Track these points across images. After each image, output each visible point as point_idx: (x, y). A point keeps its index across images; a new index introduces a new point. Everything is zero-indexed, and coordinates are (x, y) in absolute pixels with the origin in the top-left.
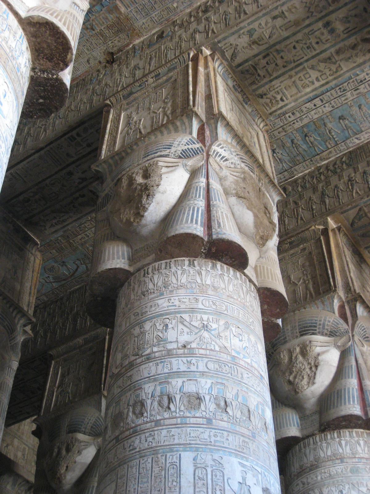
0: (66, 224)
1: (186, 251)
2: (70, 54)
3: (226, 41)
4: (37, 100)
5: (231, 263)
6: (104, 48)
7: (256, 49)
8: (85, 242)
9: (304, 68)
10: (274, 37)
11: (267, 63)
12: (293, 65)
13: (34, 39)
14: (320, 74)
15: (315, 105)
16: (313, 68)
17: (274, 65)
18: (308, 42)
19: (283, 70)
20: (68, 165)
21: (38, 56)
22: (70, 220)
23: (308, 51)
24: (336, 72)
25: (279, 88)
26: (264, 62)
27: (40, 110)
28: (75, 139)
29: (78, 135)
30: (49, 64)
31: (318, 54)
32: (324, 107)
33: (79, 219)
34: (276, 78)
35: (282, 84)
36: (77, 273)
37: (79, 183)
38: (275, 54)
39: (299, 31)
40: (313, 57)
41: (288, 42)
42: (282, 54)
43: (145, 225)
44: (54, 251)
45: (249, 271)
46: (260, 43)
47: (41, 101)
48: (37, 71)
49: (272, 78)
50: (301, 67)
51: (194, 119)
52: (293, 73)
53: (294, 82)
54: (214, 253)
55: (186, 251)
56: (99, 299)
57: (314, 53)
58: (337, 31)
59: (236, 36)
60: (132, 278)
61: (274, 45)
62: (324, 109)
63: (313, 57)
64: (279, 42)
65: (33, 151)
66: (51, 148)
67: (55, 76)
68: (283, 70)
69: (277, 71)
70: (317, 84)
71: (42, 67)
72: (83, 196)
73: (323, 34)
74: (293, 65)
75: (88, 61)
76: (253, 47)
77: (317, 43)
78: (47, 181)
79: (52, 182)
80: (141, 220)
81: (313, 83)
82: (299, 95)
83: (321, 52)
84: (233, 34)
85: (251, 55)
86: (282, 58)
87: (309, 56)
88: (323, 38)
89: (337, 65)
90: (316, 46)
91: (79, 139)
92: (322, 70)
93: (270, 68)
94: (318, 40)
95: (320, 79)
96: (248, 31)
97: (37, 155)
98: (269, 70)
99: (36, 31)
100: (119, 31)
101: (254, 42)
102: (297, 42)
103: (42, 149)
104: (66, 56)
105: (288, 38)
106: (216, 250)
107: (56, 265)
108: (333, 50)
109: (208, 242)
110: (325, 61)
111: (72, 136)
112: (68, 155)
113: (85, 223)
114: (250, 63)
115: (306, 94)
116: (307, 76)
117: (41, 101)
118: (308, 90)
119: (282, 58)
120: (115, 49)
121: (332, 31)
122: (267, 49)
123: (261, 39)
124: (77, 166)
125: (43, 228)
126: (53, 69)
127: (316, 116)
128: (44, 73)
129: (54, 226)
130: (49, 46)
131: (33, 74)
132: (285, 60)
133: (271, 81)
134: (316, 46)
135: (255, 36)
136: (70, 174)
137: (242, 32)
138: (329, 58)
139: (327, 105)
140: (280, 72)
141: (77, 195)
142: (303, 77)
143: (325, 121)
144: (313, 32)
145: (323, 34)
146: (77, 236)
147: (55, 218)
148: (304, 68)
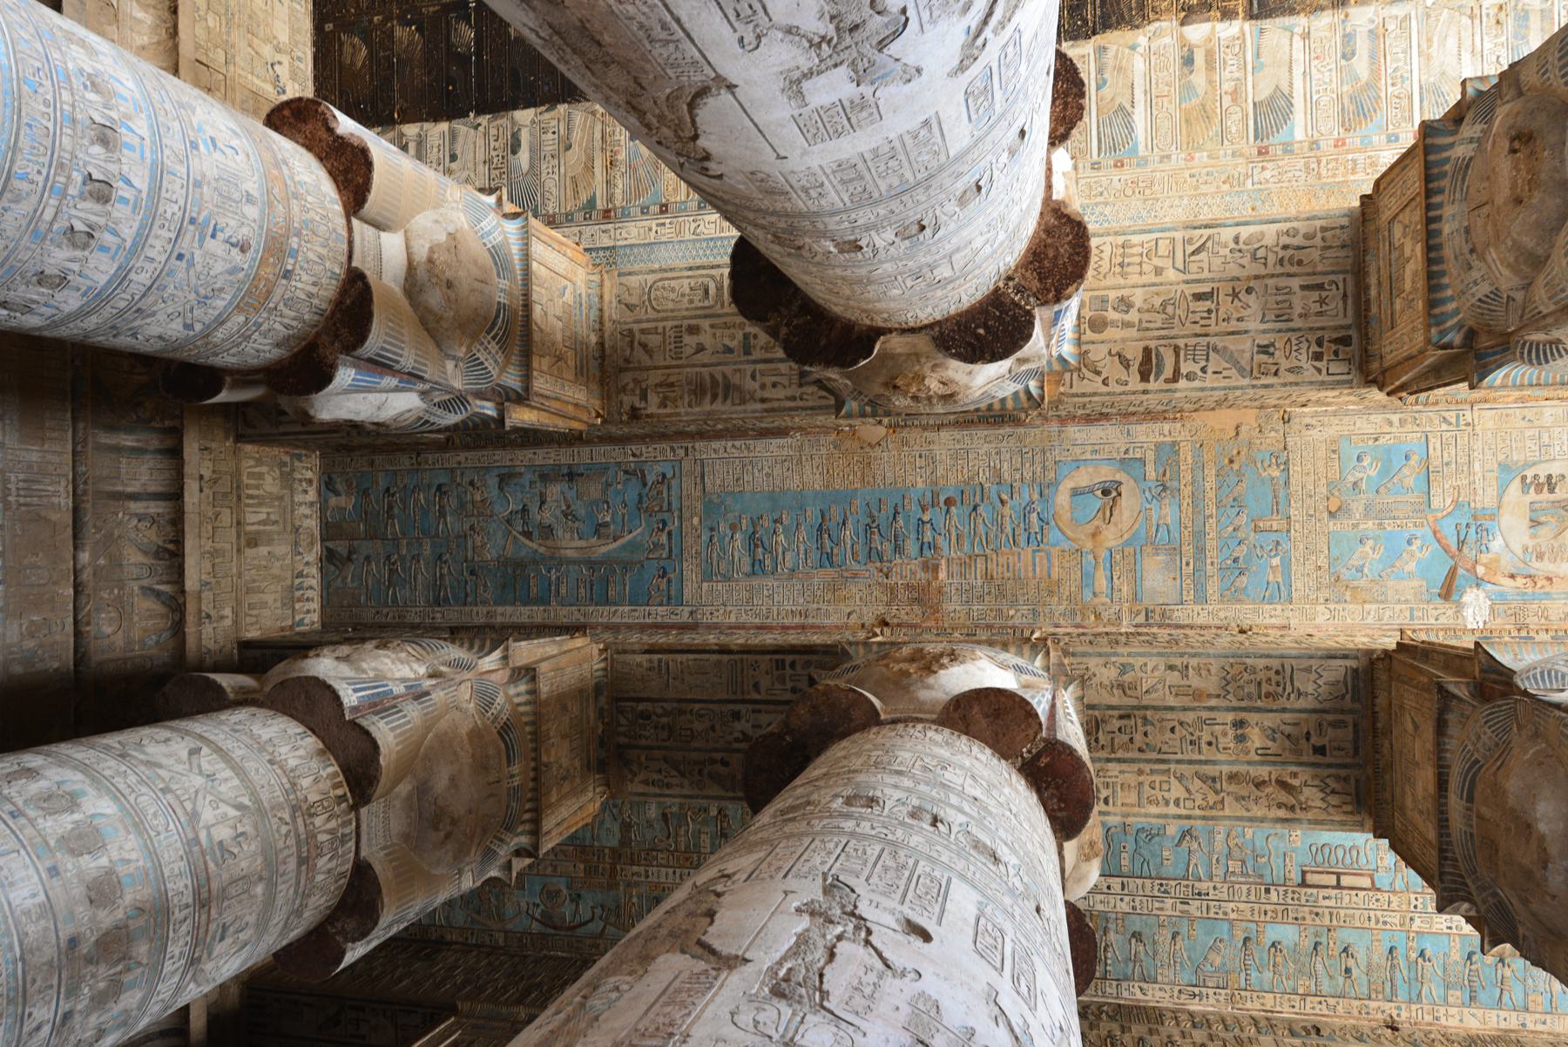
0: (667, 792)
1: (997, 735)
2: (1075, 285)
3: (1084, 660)
4: (978, 327)
5: (1053, 810)
6: (881, 609)
7: (1116, 699)
8: (637, 884)
9: (1169, 770)
10: (1154, 695)
11: (1120, 729)
12: (1154, 755)
13: (1044, 236)
14: (1187, 796)
15: (1109, 888)
16: (1180, 779)
17: (1126, 738)
18: (1198, 733)
19: (1137, 755)
20: (744, 701)
21: (1031, 262)
22: (677, 791)
23: (1190, 748)
24: (1211, 808)
25: (1114, 780)
26: (1116, 724)
27: (970, 344)
28: (784, 669)
29: (793, 665)
30: (1035, 285)
31: (1200, 762)
32: (1122, 900)
33: (690, 797)
34: (1119, 760)
35: (1121, 776)
36: (581, 931)
37: (737, 740)
38: (1139, 722)
39: (1194, 709)
40: (1191, 762)
41: (1169, 715)
42: (1149, 728)
43: (929, 687)
44: (582, 866)
45: (1070, 847)
46: (1128, 692)
47: (981, 331)
48: (1011, 284)
49: (1113, 756)
50: (1164, 767)
51: (1040, 657)
52: (1147, 768)
53: (1140, 784)
54: (1039, 768)
55: (997, 735)
56: (788, 738)
57: (1196, 757)
58: (1249, 744)
59: (1101, 660)
60: (875, 729)
61: (1146, 708)
62: (1118, 902)
63: (1191, 762)
64: (1155, 708)
65: (716, 648)
66: (742, 660)
67: (1028, 307)
68: (1137, 755)
69: (1128, 750)
70: (1172, 810)
71: (1023, 283)
72: (725, 763)
73: (1225, 734)
74: (1154, 755)
75: (849, 614)
76: (1115, 690)
77: (1210, 744)
78: (697, 706)
79: (702, 712)
80: (928, 676)
81: (1167, 803)
82: (1136, 809)
83: (1206, 762)
84: (1100, 655)
85: (1104, 702)
86: (1146, 734)
87: (1185, 757)
88: (1223, 742)
89: (1220, 798)
90: (1204, 746)
91: (788, 671)
92: (1193, 791)
93: (1123, 738)
94: (1214, 741)
95: (1182, 804)
96: (1122, 665)
97: (715, 657)
98: (1116, 741)
99: (1054, 226)
100: (918, 601)
101: (1121, 686)
102: (1181, 724)
103: (730, 652)
104: (1068, 285)
105: (1172, 709)
106: (1047, 765)
107: (565, 891)
108: (1226, 769)
109: (1044, 740)
110: (1204, 778)
111: (783, 661)
112: (756, 686)
113: (661, 851)
114: (1096, 713)
115: (1146, 815)
116: (1165, 787)
117: (981, 331)
118: (1153, 810)
119: (1146, 734)
120: (895, 621)
121: (1241, 739)
122: (1133, 707)
123: (1132, 686)
124: (754, 711)
125: (630, 777)
126: (1035, 295)
127: (1100, 907)
129: (648, 784)
130: (1056, 257)
131: (1001, 284)
132: (1147, 740)
133: (1108, 760)
134: (1204, 746)
135: (1127, 678)
136: (736, 716)
137: (1113, 659)
138: (1214, 779)
139: (1126, 899)
140: (1129, 755)
141: (718, 756)
142: (1157, 784)
143: (1110, 925)
144: (1211, 722)
145: (1225, 734)
146: (633, 864)
147: (660, 771)
148: (1169, 770)
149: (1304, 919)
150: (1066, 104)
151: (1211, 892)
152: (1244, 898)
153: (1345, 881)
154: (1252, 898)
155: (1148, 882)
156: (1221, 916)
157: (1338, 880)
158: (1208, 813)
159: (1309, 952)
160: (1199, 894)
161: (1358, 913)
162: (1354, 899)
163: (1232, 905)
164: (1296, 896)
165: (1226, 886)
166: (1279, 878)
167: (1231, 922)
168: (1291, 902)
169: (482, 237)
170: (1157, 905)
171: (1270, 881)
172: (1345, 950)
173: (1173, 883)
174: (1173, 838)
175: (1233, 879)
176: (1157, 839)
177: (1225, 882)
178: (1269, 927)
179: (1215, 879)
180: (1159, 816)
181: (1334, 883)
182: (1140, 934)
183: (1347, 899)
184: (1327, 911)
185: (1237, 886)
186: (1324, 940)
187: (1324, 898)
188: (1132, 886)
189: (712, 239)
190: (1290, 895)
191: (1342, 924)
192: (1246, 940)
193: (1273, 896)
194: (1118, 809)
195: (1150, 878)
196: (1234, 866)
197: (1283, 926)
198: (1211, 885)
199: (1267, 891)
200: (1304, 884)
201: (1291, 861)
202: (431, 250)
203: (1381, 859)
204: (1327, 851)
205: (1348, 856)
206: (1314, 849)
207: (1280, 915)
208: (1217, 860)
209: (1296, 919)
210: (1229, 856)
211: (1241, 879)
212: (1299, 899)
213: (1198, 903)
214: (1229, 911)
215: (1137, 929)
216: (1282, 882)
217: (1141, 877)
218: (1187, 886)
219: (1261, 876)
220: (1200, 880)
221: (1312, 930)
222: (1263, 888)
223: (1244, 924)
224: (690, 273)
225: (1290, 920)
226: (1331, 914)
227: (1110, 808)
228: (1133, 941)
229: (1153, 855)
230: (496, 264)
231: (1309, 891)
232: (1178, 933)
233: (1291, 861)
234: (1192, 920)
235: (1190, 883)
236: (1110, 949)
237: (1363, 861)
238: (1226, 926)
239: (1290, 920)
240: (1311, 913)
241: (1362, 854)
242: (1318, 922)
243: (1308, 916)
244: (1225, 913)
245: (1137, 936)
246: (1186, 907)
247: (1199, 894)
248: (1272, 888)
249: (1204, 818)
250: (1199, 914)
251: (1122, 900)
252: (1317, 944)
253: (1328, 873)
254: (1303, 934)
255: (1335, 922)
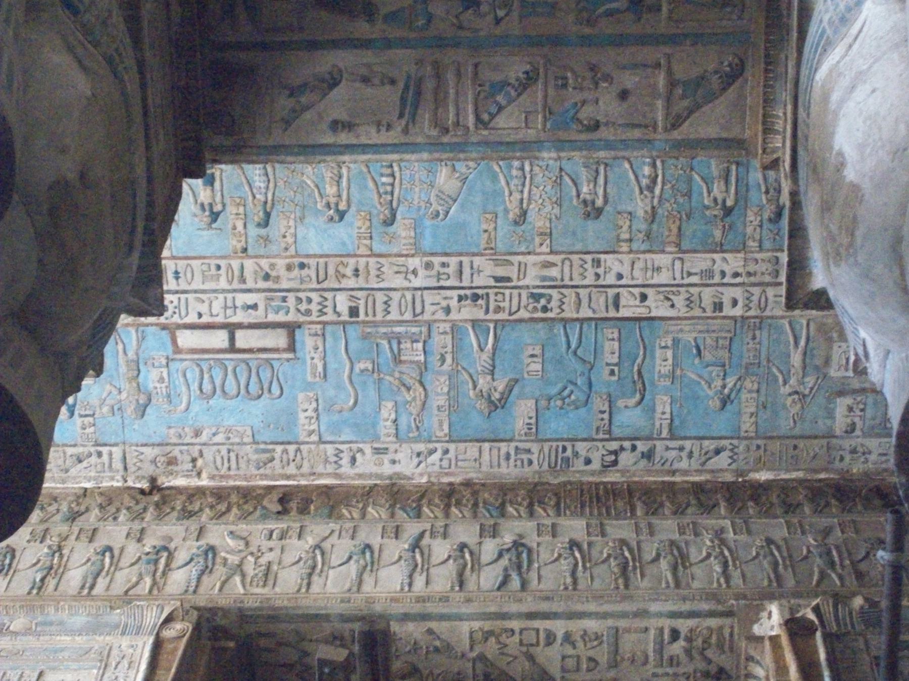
15: (644, 297)
32: (620, 276)
62: (625, 270)
115: (605, 616)
127: (662, 260)
139: (611, 279)
149: (289, 268)
151: (454, 303)
152: (396, 296)
153: (220, 339)
154: (380, 297)
155: (570, 313)
156: (437, 260)
157: (232, 339)
158: (500, 624)
159: (279, 207)
160: (476, 297)
161: (197, 285)
162: (204, 308)
163: (417, 282)
164: (303, 307)
165: (426, 317)
166: (334, 334)
167: (417, 250)
168: (314, 296)
170: (554, 272)
171: (350, 330)
172: (215, 216)
173: (523, 314)
174: (520, 397)
175: (414, 330)
176: (554, 391)
177: (429, 325)
178: (350, 249)
179: (447, 327)
180: (581, 615)
181: (239, 334)
182: (587, 215)
183: (217, 307)
184: (250, 284)
185: (408, 316)
186: (253, 231)
187: (255, 307)
188: (600, 301)
190: (314, 307)
191: (223, 263)
192: (390, 221)
193: (343, 303)
194: (653, 624)
195: (565, 321)
196: (414, 353)
197: (326, 250)
198: (454, 316)
199: (354, 312)
200: (291, 328)
201: (314, 367)
203: (161, 380)
204: (254, 388)
205: (218, 382)
206: (276, 390)
207: (331, 271)
208: (443, 360)
209: (302, 266)
210: (424, 367)
211: (398, 329)
212: (299, 300)
213: (479, 281)
214: (421, 272)
215: (591, 225)
216: (329, 328)
217: (582, 321)
218: (498, 309)
219: (365, 337)
220: (475, 323)
221: (274, 249)
222: (362, 317)
223: (395, 250)
225: (312, 262)
226: (243, 280)
227: (667, 624)
228: (599, 202)
229: (560, 361)
231: (281, 318)
232: (516, 223)
233: (314, 367)
234: (491, 251)
235: (491, 316)
236: (645, 182)
237: (193, 375)
238: (427, 243)
239: (312, 262)
240: (277, 279)
241: (195, 387)
242: (264, 263)
243: (283, 272)
244: (428, 266)
245: (593, 212)
246: (501, 272)
247: (476, 297)
248: (345, 317)
249: (504, 616)
250: (477, 261)
251: (620, 276)
252: (265, 222)
253: (250, 351)
254: (290, 240)
255: (235, 264)
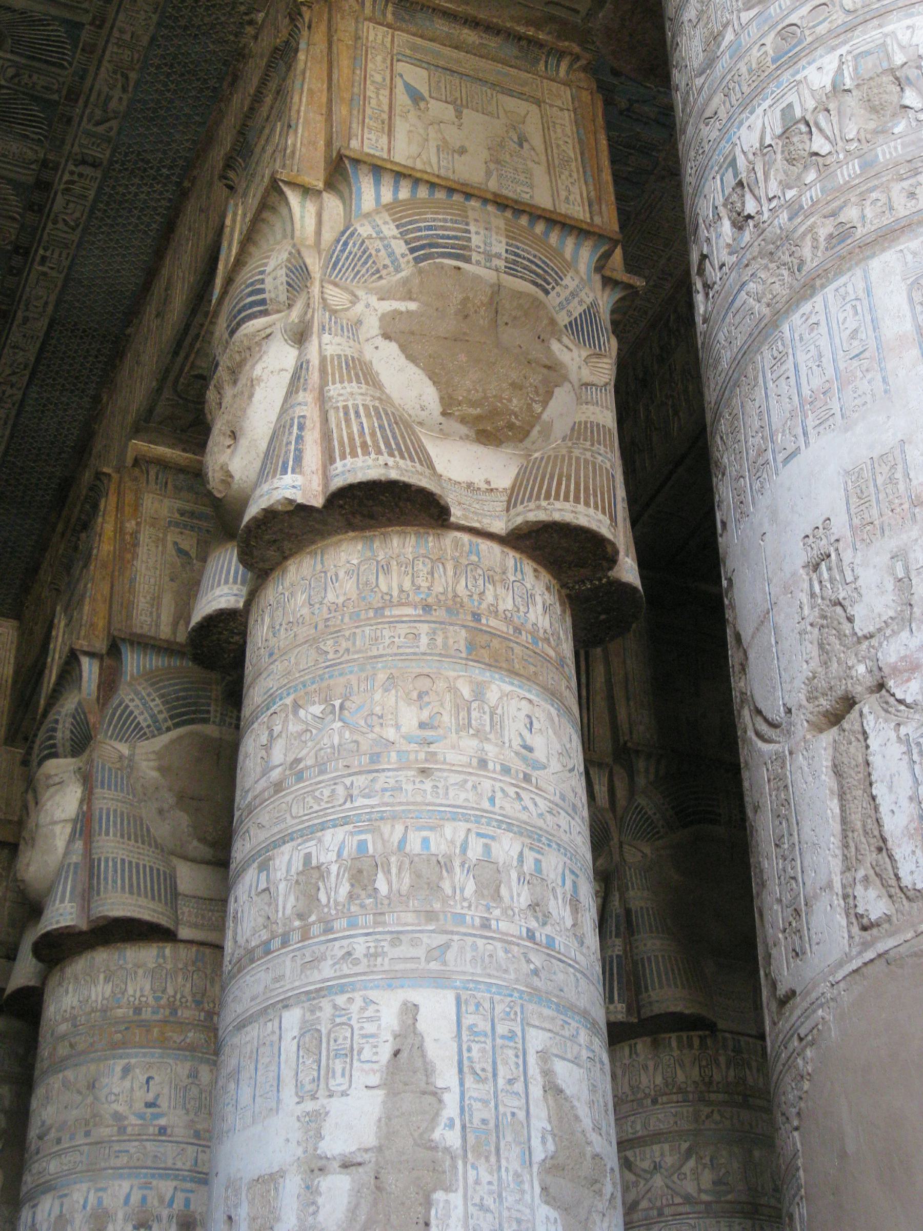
47: (603, 617)
67: (604, 580)
128: (585, 584)
150: (408, 500)
169: (159, 729)
189: (92, 212)
202: (200, 840)
224: (182, 354)
230: (192, 722)
